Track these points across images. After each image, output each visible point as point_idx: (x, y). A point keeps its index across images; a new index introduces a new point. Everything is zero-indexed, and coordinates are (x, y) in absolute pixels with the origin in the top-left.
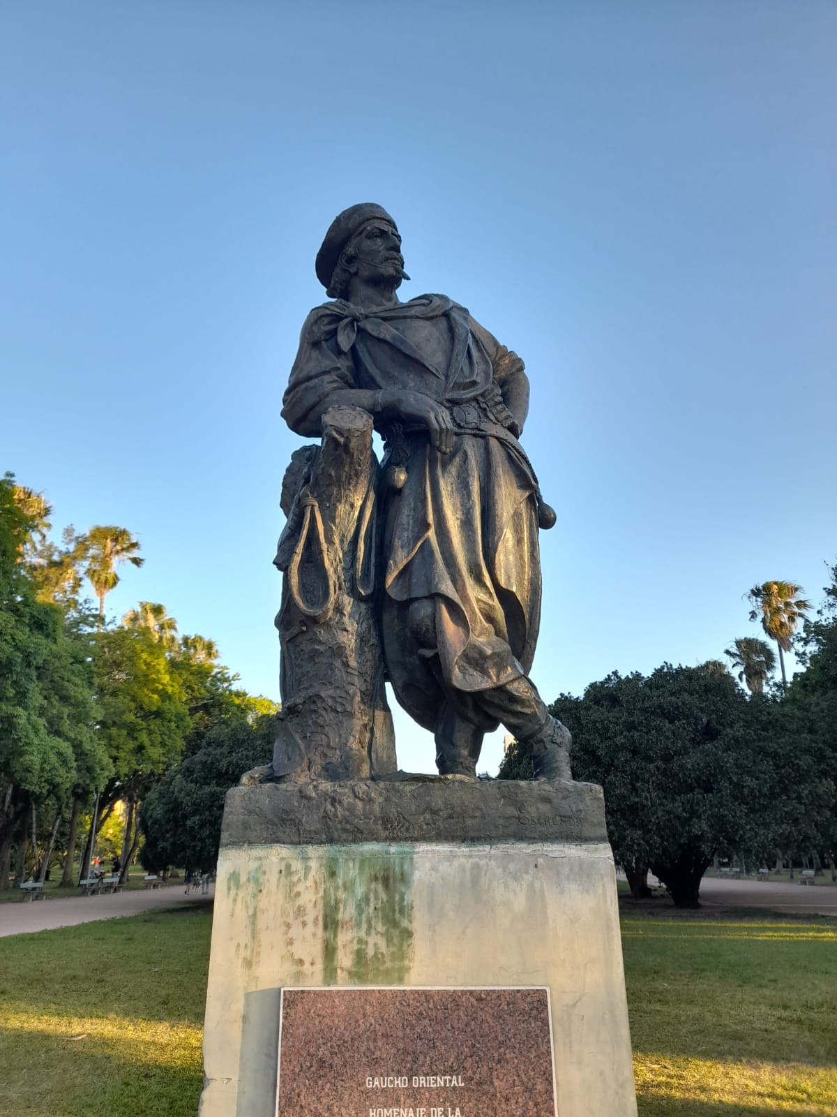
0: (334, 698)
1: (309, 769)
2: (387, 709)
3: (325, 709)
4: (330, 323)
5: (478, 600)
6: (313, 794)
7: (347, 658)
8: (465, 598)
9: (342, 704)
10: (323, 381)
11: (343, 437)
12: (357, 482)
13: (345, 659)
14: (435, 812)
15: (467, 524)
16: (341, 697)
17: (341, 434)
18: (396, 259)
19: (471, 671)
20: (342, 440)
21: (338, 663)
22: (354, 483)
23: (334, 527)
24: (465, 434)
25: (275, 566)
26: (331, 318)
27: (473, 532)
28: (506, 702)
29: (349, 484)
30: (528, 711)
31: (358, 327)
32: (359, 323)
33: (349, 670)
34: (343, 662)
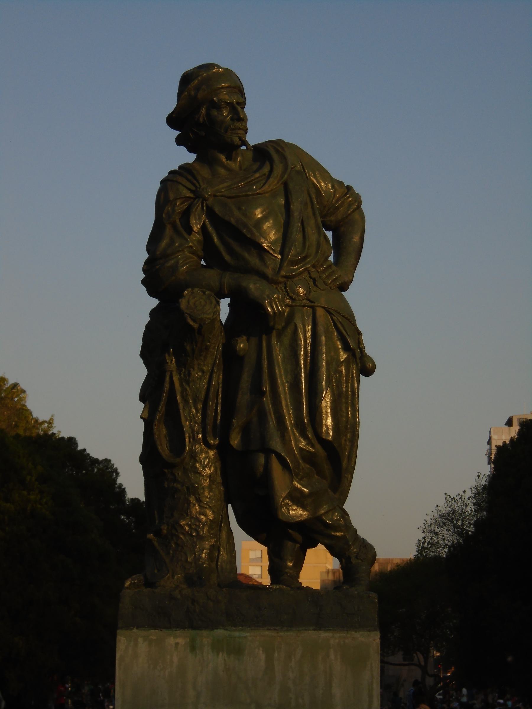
0: (190, 526)
1: (173, 576)
2: (230, 533)
3: (183, 534)
4: (182, 203)
5: (301, 450)
6: (179, 596)
7: (199, 495)
8: (290, 451)
9: (196, 530)
10: (177, 262)
11: (197, 323)
13: (197, 497)
15: (295, 385)
16: (196, 525)
17: (194, 321)
18: (240, 129)
20: (196, 326)
21: (192, 499)
23: (188, 389)
24: (296, 306)
25: (142, 420)
26: (184, 199)
27: (300, 389)
30: (339, 534)
31: (206, 204)
32: (207, 202)
33: (201, 504)
34: (196, 497)
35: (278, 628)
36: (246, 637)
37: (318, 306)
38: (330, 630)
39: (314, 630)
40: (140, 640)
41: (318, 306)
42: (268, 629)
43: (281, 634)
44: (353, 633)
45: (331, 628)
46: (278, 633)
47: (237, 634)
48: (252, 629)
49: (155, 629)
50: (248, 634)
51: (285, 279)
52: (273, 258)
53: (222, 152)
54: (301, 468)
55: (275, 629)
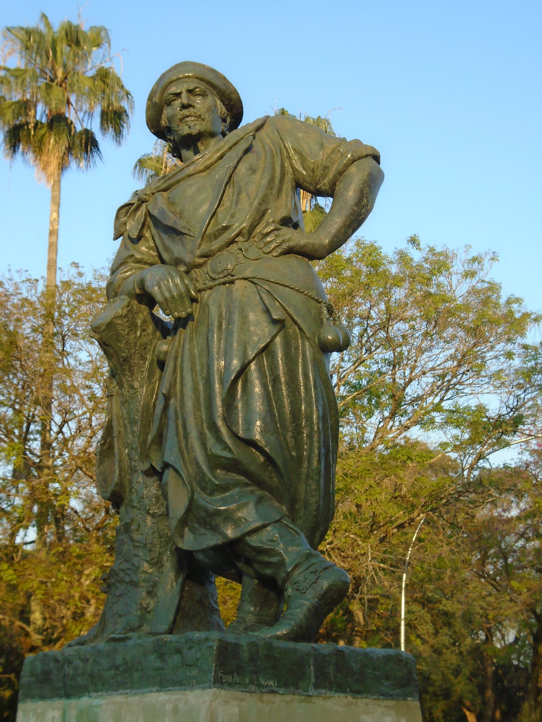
12: (130, 366)
14: (117, 668)
19: (202, 530)
22: (127, 367)
28: (254, 554)
29: (124, 370)
35: (128, 691)
36: (101, 706)
37: (237, 279)
38: (169, 690)
39: (157, 691)
40: (31, 714)
41: (237, 279)
42: (121, 694)
43: (130, 699)
44: (189, 692)
45: (171, 688)
46: (127, 698)
47: (96, 702)
48: (109, 695)
49: (42, 700)
50: (103, 702)
51: (205, 259)
52: (192, 238)
53: (188, 148)
54: (207, 479)
55: (126, 694)
